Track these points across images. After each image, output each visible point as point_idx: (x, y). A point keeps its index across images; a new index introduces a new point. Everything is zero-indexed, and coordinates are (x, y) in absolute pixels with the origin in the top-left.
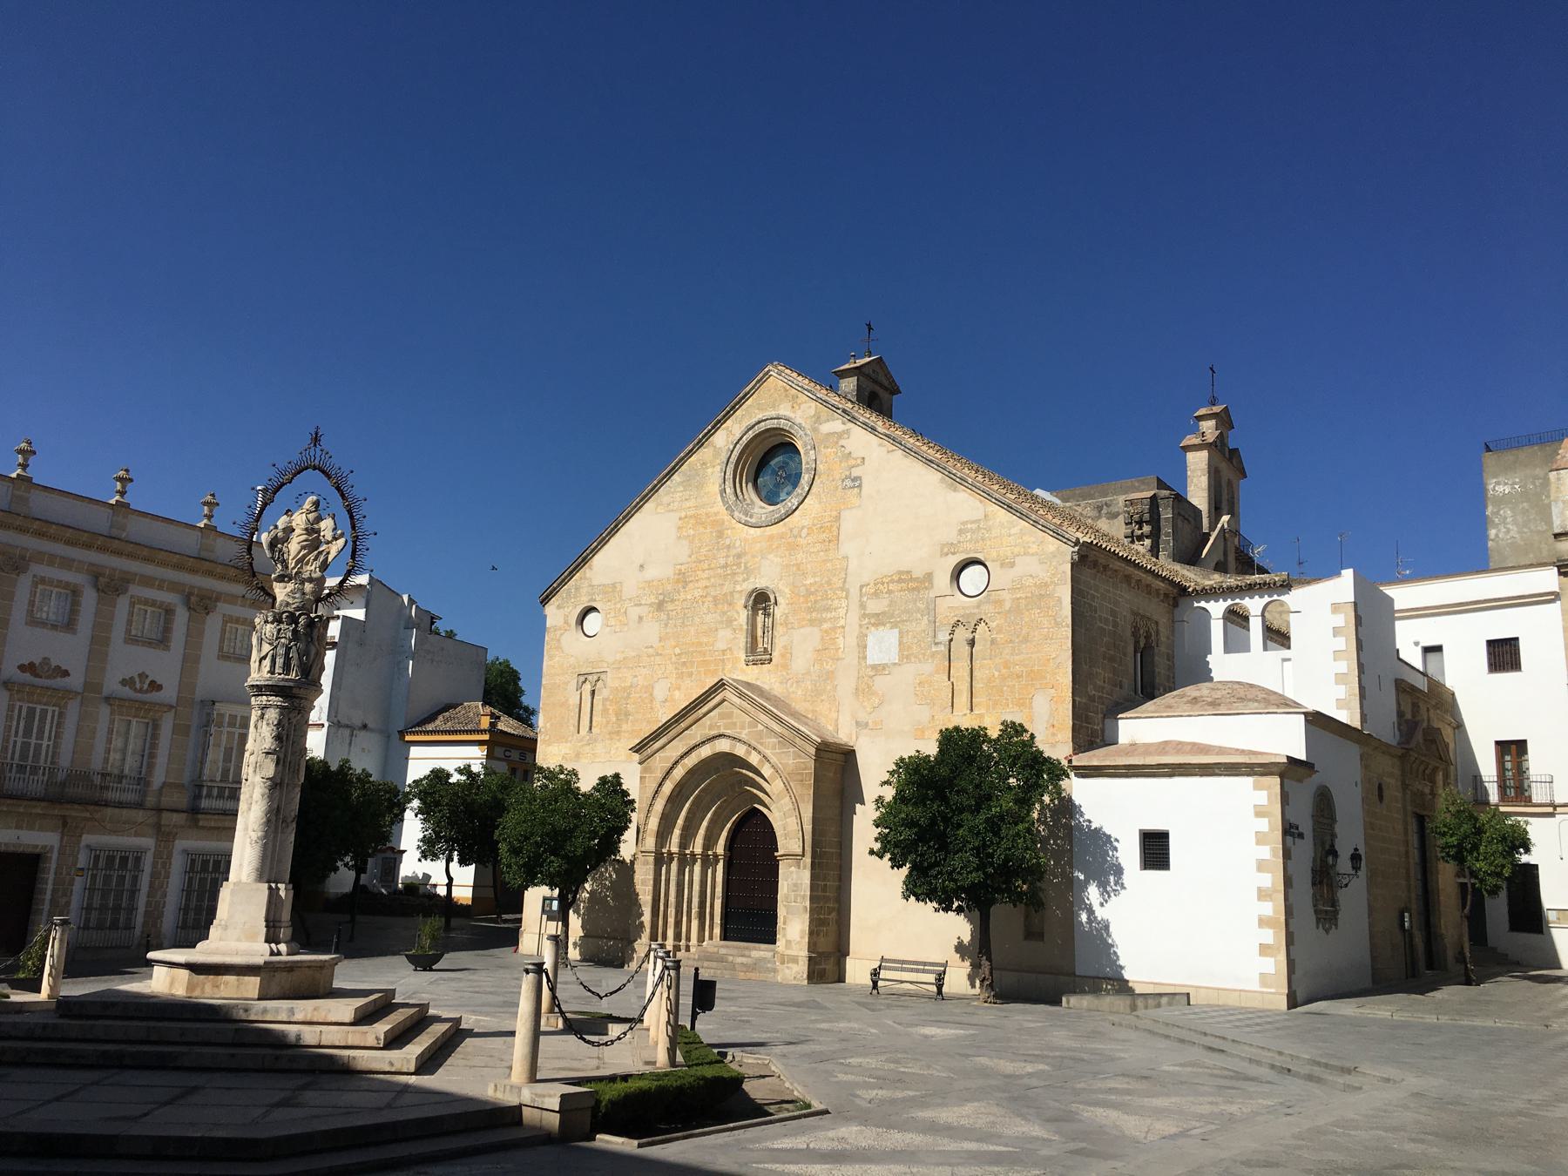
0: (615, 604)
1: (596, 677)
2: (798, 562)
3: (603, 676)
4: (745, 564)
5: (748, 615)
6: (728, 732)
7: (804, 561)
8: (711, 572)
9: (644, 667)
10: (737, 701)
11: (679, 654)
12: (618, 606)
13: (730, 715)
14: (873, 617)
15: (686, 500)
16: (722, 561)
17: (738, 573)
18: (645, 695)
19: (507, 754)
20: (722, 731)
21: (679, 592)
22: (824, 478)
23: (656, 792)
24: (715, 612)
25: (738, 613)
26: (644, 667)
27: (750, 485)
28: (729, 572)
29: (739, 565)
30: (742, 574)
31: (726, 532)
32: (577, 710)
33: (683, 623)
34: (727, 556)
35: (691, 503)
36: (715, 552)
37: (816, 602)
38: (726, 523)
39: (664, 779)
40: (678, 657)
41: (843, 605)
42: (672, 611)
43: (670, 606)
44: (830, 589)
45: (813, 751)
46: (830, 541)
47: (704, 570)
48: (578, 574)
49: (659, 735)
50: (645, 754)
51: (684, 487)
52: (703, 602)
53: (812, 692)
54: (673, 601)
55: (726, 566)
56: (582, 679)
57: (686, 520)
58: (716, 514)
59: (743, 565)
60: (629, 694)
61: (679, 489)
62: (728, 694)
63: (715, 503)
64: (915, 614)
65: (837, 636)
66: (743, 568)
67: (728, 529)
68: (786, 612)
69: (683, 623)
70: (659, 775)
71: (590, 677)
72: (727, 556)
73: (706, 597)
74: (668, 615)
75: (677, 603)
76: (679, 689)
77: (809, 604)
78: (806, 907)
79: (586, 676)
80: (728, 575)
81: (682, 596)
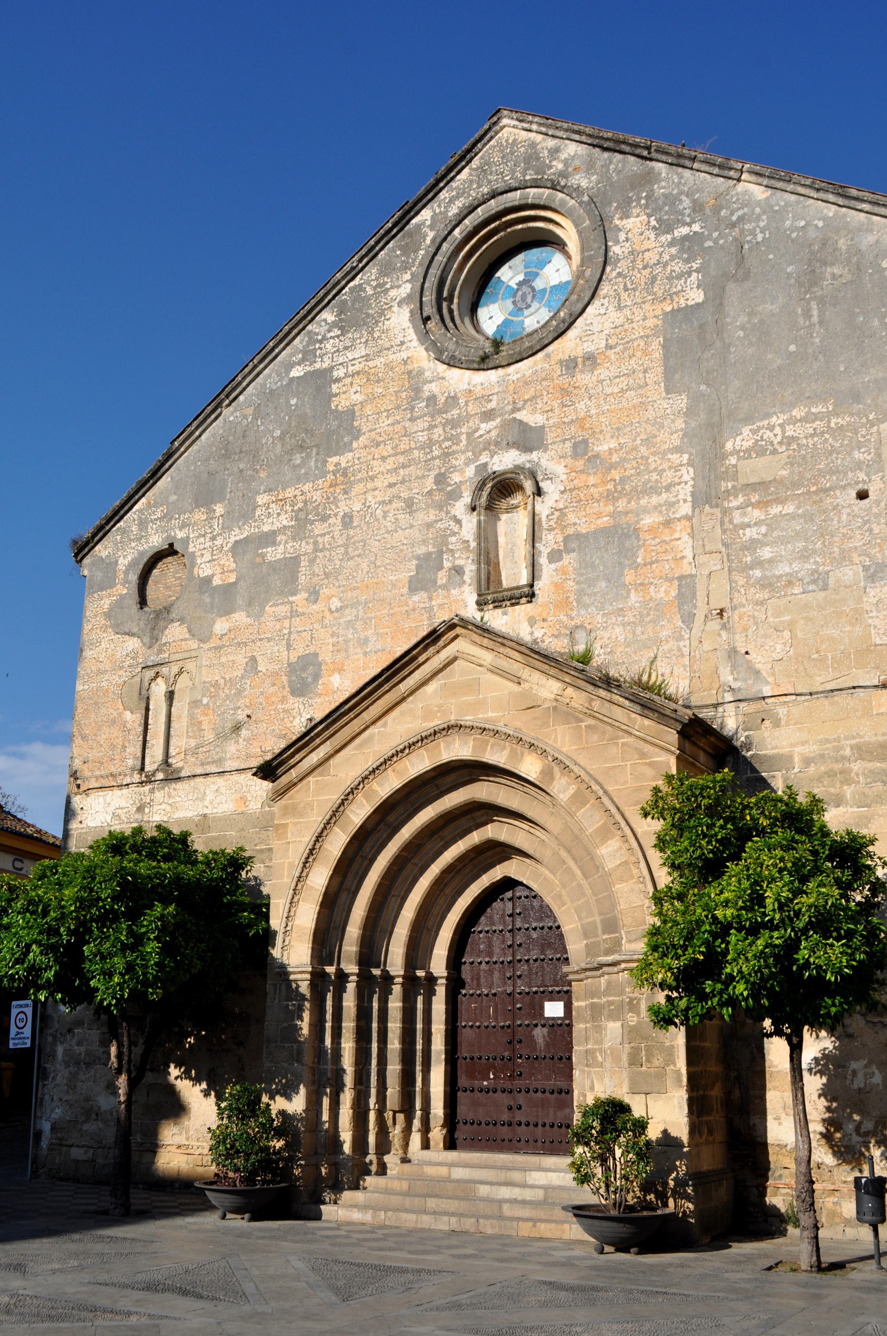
0: (213, 538)
1: (175, 669)
2: (582, 415)
3: (190, 666)
4: (469, 435)
5: (479, 522)
6: (468, 719)
7: (593, 412)
8: (401, 459)
9: (269, 640)
10: (487, 657)
11: (337, 611)
12: (219, 542)
13: (473, 686)
14: (755, 491)
15: (346, 348)
16: (422, 437)
17: (454, 453)
18: (272, 690)
19: (18, 865)
20: (453, 719)
21: (336, 501)
22: (623, 266)
23: (311, 851)
24: (412, 526)
25: (458, 522)
26: (269, 640)
27: (467, 320)
28: (436, 453)
29: (455, 439)
30: (463, 452)
31: (426, 388)
32: (140, 729)
33: (346, 552)
34: (431, 427)
35: (360, 351)
36: (407, 424)
37: (623, 480)
38: (428, 374)
39: (327, 825)
40: (336, 615)
41: (686, 477)
42: (324, 535)
43: (319, 528)
44: (653, 454)
45: (672, 737)
46: (645, 371)
47: (384, 459)
48: (143, 500)
49: (312, 740)
50: (284, 780)
51: (340, 328)
52: (385, 513)
53: (628, 645)
54: (324, 518)
55: (431, 443)
56: (150, 673)
57: (348, 381)
58: (405, 362)
59: (464, 437)
60: (239, 692)
61: (332, 334)
62: (462, 645)
63: (402, 343)
64: (850, 474)
65: (677, 535)
66: (464, 442)
67: (430, 382)
68: (561, 506)
69: (346, 552)
70: (316, 819)
71: (164, 670)
72: (431, 427)
73: (390, 502)
74: (316, 543)
75: (331, 521)
76: (340, 671)
77: (610, 486)
78: (678, 1072)
79: (156, 669)
80: (433, 458)
81: (343, 507)
